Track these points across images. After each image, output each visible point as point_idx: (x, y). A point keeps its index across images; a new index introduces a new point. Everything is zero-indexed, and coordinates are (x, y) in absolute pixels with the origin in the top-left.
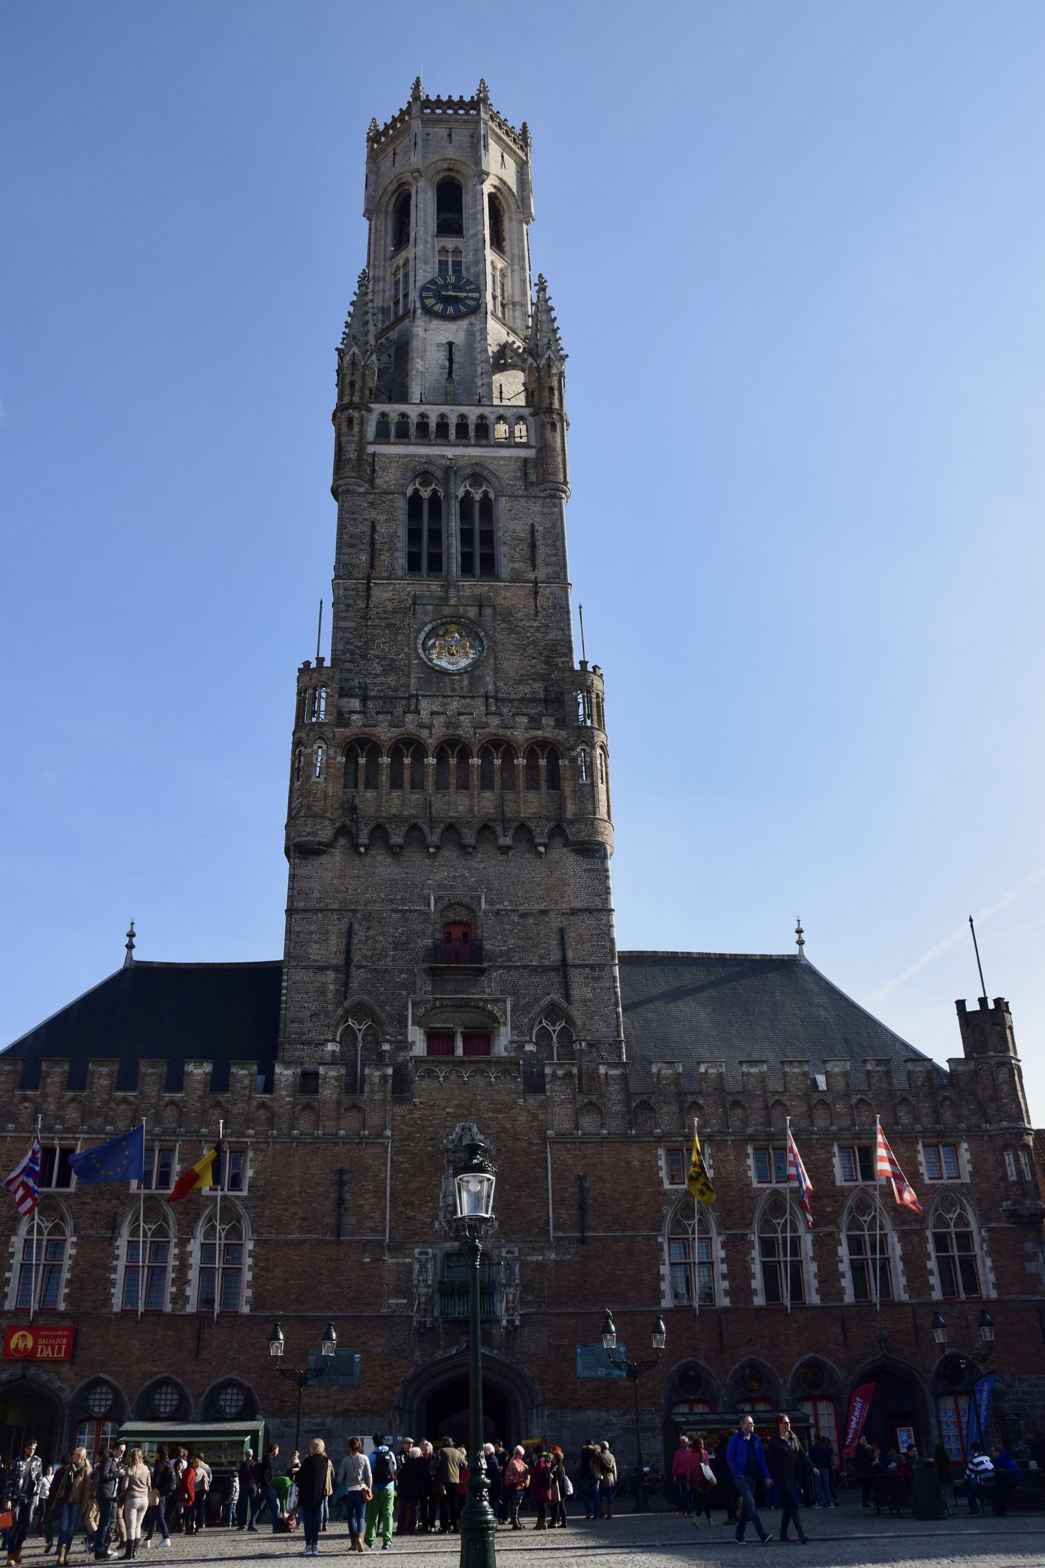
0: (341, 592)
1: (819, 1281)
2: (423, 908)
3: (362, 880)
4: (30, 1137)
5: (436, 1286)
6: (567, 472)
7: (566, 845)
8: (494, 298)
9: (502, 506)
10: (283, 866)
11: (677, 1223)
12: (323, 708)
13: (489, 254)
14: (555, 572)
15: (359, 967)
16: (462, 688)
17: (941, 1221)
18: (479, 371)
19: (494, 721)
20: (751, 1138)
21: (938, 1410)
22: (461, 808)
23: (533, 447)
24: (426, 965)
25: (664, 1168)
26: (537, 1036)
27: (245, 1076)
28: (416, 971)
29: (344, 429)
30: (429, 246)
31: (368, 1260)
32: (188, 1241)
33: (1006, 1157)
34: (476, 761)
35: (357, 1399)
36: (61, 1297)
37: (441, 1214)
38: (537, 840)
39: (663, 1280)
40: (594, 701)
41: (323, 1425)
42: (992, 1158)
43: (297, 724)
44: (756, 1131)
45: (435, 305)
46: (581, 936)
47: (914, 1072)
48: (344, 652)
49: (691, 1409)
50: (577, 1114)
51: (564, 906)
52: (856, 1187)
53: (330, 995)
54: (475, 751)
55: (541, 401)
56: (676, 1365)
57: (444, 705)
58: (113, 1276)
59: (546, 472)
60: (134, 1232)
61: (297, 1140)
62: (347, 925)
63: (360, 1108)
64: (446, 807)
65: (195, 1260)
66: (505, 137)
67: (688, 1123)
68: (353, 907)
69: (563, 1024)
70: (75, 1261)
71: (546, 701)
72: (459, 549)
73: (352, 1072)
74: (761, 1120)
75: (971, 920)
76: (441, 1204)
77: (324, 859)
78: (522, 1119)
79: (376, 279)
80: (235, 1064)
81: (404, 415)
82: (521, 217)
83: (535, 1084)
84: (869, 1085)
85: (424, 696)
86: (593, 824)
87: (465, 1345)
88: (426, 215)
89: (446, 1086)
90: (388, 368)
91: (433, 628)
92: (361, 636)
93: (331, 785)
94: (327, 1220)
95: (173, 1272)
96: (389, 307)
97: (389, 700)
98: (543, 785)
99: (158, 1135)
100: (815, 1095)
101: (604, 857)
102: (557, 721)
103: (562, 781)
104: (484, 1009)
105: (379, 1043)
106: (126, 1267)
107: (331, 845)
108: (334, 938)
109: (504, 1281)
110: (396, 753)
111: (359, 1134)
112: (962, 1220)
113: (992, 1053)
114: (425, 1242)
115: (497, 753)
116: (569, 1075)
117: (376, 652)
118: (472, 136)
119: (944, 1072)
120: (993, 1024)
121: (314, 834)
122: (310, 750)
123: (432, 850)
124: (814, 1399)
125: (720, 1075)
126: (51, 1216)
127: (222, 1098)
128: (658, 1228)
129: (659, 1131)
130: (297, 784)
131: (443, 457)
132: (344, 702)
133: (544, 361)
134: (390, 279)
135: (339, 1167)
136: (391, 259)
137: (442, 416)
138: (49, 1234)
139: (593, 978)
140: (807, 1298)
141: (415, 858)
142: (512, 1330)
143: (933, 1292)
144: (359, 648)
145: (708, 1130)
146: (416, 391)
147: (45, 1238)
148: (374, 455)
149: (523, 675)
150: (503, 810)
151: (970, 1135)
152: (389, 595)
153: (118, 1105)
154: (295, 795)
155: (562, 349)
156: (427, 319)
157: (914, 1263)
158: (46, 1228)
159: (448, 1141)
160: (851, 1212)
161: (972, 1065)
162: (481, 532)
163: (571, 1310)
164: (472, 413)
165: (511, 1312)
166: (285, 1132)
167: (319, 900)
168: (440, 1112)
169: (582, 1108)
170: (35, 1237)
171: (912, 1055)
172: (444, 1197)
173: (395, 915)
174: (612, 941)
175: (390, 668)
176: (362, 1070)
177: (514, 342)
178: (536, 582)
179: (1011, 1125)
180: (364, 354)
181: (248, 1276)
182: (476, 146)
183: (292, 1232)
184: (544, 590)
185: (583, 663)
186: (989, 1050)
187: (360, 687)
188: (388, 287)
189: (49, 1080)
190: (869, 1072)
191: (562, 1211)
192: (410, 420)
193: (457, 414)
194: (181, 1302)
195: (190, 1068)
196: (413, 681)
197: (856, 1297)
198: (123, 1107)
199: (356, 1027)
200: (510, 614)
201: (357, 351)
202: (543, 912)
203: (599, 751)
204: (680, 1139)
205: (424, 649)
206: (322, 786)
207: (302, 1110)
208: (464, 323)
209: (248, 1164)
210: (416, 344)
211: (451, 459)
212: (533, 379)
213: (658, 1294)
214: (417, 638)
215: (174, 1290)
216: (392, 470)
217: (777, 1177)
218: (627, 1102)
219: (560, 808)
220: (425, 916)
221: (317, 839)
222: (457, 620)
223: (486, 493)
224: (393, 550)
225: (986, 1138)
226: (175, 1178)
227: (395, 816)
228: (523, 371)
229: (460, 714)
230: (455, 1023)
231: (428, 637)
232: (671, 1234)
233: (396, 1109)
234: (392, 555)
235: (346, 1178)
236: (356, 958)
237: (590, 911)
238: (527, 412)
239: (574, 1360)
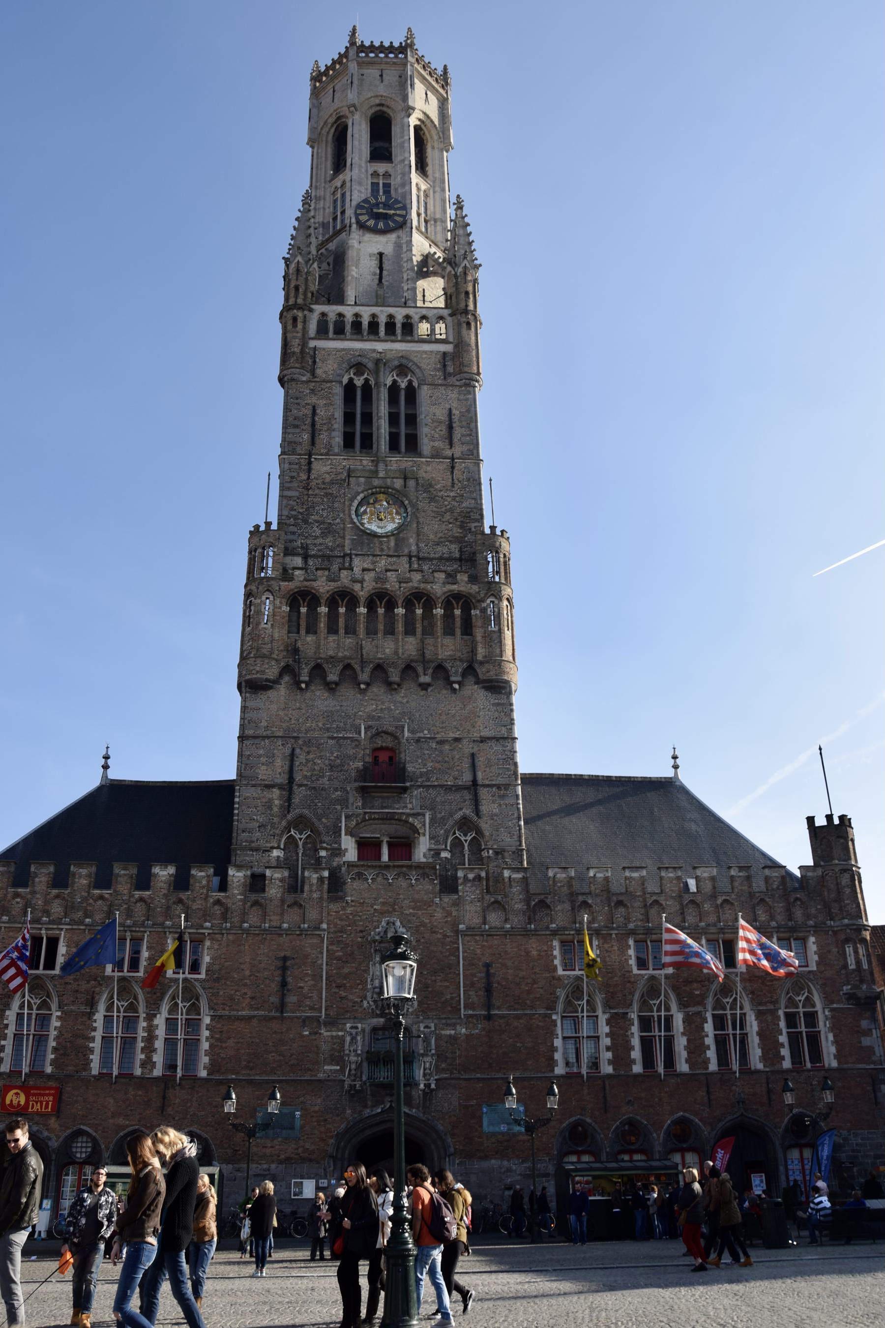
0: (287, 466)
1: (688, 1053)
2: (355, 735)
3: (303, 711)
4: (21, 928)
5: (365, 1055)
6: (481, 364)
7: (477, 683)
8: (419, 215)
9: (424, 393)
10: (236, 699)
11: (568, 1003)
12: (270, 565)
13: (415, 177)
14: (469, 450)
15: (300, 786)
16: (389, 548)
17: (791, 1003)
18: (405, 277)
19: (417, 577)
20: (632, 932)
21: (786, 1161)
22: (387, 651)
23: (450, 343)
24: (357, 784)
25: (558, 957)
26: (451, 845)
27: (203, 877)
28: (348, 789)
29: (290, 327)
30: (363, 170)
31: (307, 1033)
32: (155, 1016)
33: (847, 949)
34: (400, 611)
35: (297, 1149)
36: (48, 1062)
37: (369, 995)
38: (453, 679)
39: (557, 1051)
40: (502, 560)
41: (269, 1170)
42: (835, 950)
43: (248, 578)
44: (636, 926)
46: (489, 760)
47: (771, 877)
48: (289, 517)
49: (579, 1158)
50: (485, 911)
51: (475, 734)
53: (275, 809)
54: (400, 602)
55: (458, 303)
56: (567, 1122)
57: (374, 563)
58: (91, 1045)
59: (462, 364)
60: (109, 1008)
61: (247, 931)
62: (290, 750)
63: (301, 905)
64: (375, 650)
65: (161, 1032)
66: (428, 78)
67: (578, 919)
68: (295, 735)
70: (60, 1031)
71: (460, 560)
72: (387, 429)
73: (294, 875)
74: (641, 917)
75: (820, 749)
76: (369, 986)
77: (271, 694)
78: (439, 915)
79: (318, 199)
80: (194, 867)
81: (340, 315)
82: (442, 146)
83: (449, 885)
84: (733, 888)
85: (356, 555)
86: (500, 665)
87: (388, 1105)
88: (360, 144)
89: (374, 887)
90: (328, 274)
91: (365, 497)
92: (303, 504)
93: (277, 630)
94: (272, 999)
95: (142, 1041)
96: (329, 222)
98: (458, 631)
99: (129, 927)
100: (686, 896)
101: (510, 693)
102: (469, 577)
103: (474, 629)
104: (406, 822)
105: (316, 850)
106: (103, 1037)
107: (276, 682)
108: (279, 761)
109: (422, 1051)
110: (333, 603)
111: (299, 927)
112: (809, 1001)
113: (837, 862)
114: (355, 1018)
115: (419, 603)
116: (478, 878)
117: (316, 518)
118: (400, 77)
119: (796, 877)
120: (838, 837)
121: (263, 672)
122: (258, 601)
123: (363, 686)
124: (683, 1151)
125: (606, 879)
126: (39, 994)
127: (184, 896)
128: (552, 1007)
129: (554, 925)
130: (248, 629)
131: (374, 351)
132: (288, 559)
133: (460, 269)
134: (329, 199)
135: (282, 955)
136: (330, 181)
137: (374, 316)
138: (38, 1009)
139: (499, 796)
140: (678, 1066)
141: (347, 692)
142: (428, 1093)
143: (783, 1062)
144: (301, 514)
145: (596, 925)
146: (351, 294)
147: (34, 1012)
148: (315, 348)
149: (441, 538)
150: (424, 653)
151: (818, 930)
152: (328, 468)
153: (95, 901)
154: (246, 639)
155: (476, 259)
156: (361, 232)
157: (768, 1038)
158: (35, 1004)
159: (375, 934)
160: (716, 995)
161: (819, 872)
162: (406, 415)
163: (478, 1075)
164: (399, 314)
165: (428, 1077)
166: (237, 925)
167: (267, 728)
168: (369, 909)
169: (488, 906)
170: (26, 1011)
171: (769, 863)
172: (372, 980)
173: (331, 742)
174: (516, 765)
175: (328, 531)
176: (303, 873)
177: (435, 253)
178: (453, 459)
179: (851, 922)
180: (307, 262)
181: (205, 1045)
182: (403, 85)
183: (243, 1009)
184: (460, 465)
185: (493, 528)
186: (833, 859)
187: (302, 547)
188: (327, 205)
189: (37, 880)
190: (732, 877)
192: (346, 320)
193: (386, 314)
194: (149, 1067)
195: (156, 870)
196: (347, 542)
197: (719, 1065)
198: (100, 902)
199: (297, 836)
200: (431, 485)
201: (301, 260)
202: (457, 740)
203: (505, 603)
204: (572, 932)
205: (357, 515)
206: (269, 631)
207: (252, 906)
208: (392, 237)
209: (206, 951)
210: (351, 254)
211: (381, 353)
212: (452, 285)
213: (552, 1063)
214: (350, 505)
215: (143, 1056)
216: (330, 362)
217: (654, 965)
218: (527, 901)
219: (472, 651)
220: (357, 743)
221: (265, 677)
222: (385, 490)
223: (410, 382)
224: (330, 430)
225: (830, 933)
226: (143, 963)
227: (332, 657)
228: (443, 277)
229: (387, 571)
230: (381, 833)
231: (360, 504)
232: (564, 1012)
233: (331, 906)
234: (330, 434)
235: (288, 963)
236: (298, 777)
237: (497, 739)
238: (446, 313)
239: (481, 1118)
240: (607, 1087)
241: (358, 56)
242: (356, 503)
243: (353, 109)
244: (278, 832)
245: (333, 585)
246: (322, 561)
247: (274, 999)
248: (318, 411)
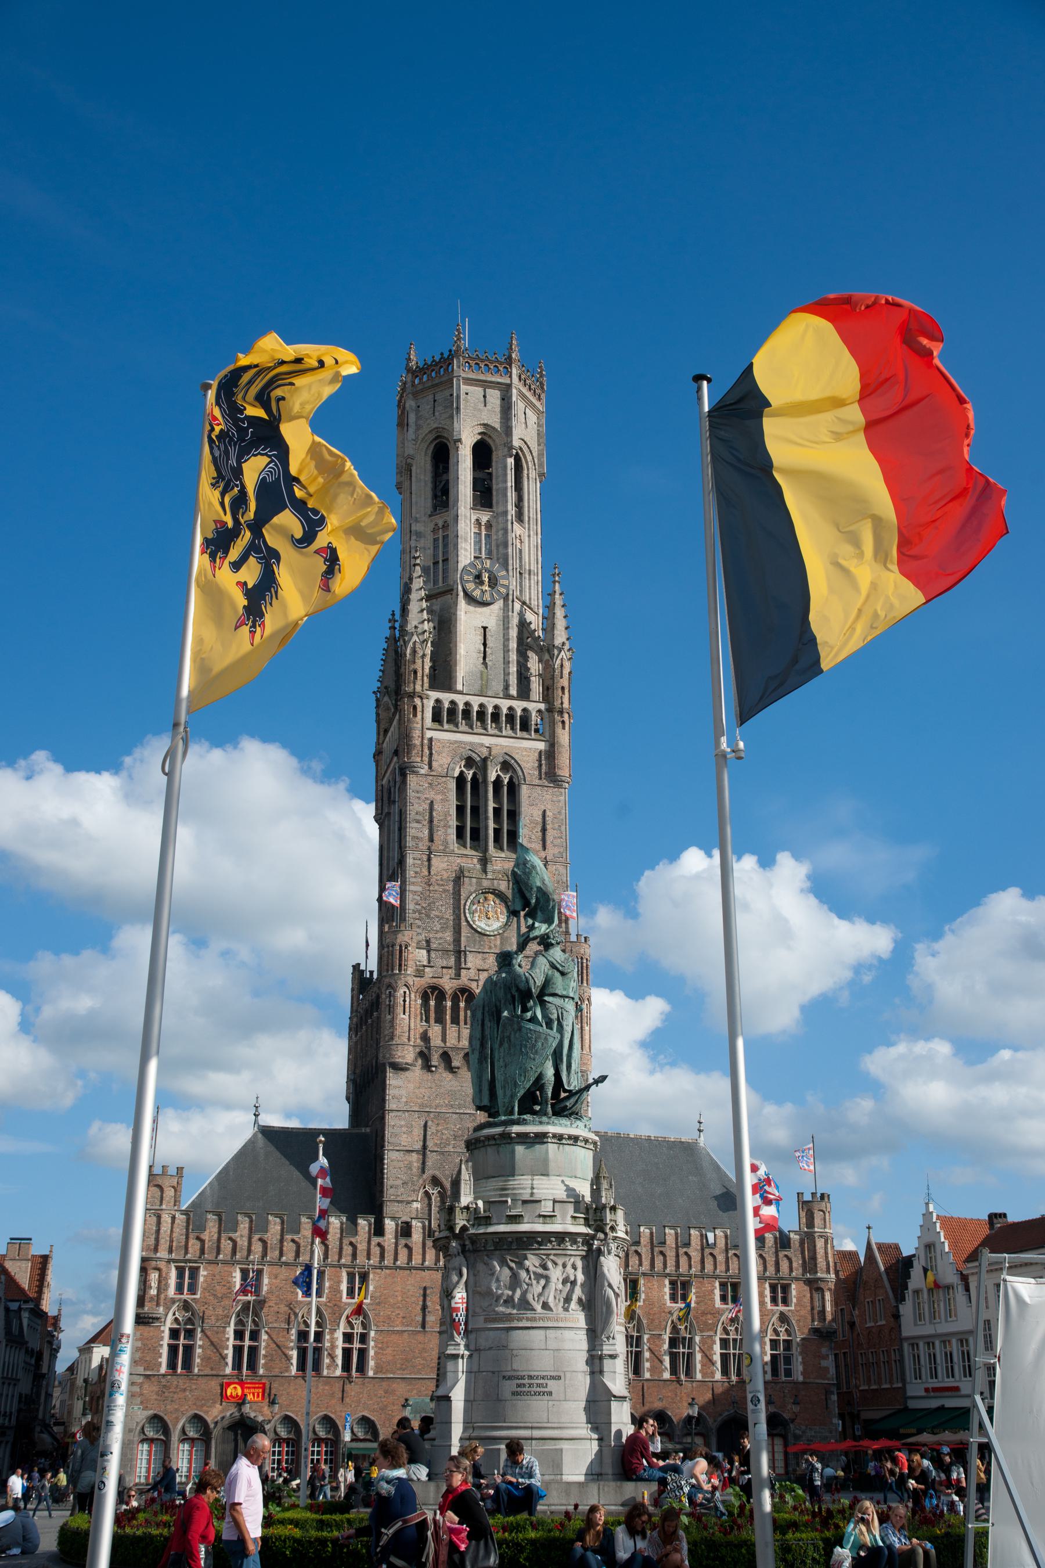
9: (524, 791)
16: (495, 946)
45: (474, 590)
53: (415, 1170)
57: (484, 959)
58: (291, 1353)
65: (340, 1343)
68: (427, 1110)
81: (453, 702)
92: (425, 899)
96: (429, 566)
110: (455, 999)
117: (437, 913)
121: (403, 1057)
131: (482, 745)
133: (558, 662)
134: (430, 538)
148: (431, 740)
151: (797, 1279)
152: (444, 865)
164: (505, 705)
183: (397, 1326)
189: (242, 1226)
196: (463, 939)
199: (431, 1192)
203: (586, 1002)
205: (470, 913)
214: (465, 904)
216: (444, 755)
221: (405, 1061)
223: (511, 778)
231: (472, 903)
235: (428, 1292)
236: (430, 1144)
240: (645, 1388)
244: (416, 1188)
245: (455, 984)
247: (420, 1318)
248: (436, 807)
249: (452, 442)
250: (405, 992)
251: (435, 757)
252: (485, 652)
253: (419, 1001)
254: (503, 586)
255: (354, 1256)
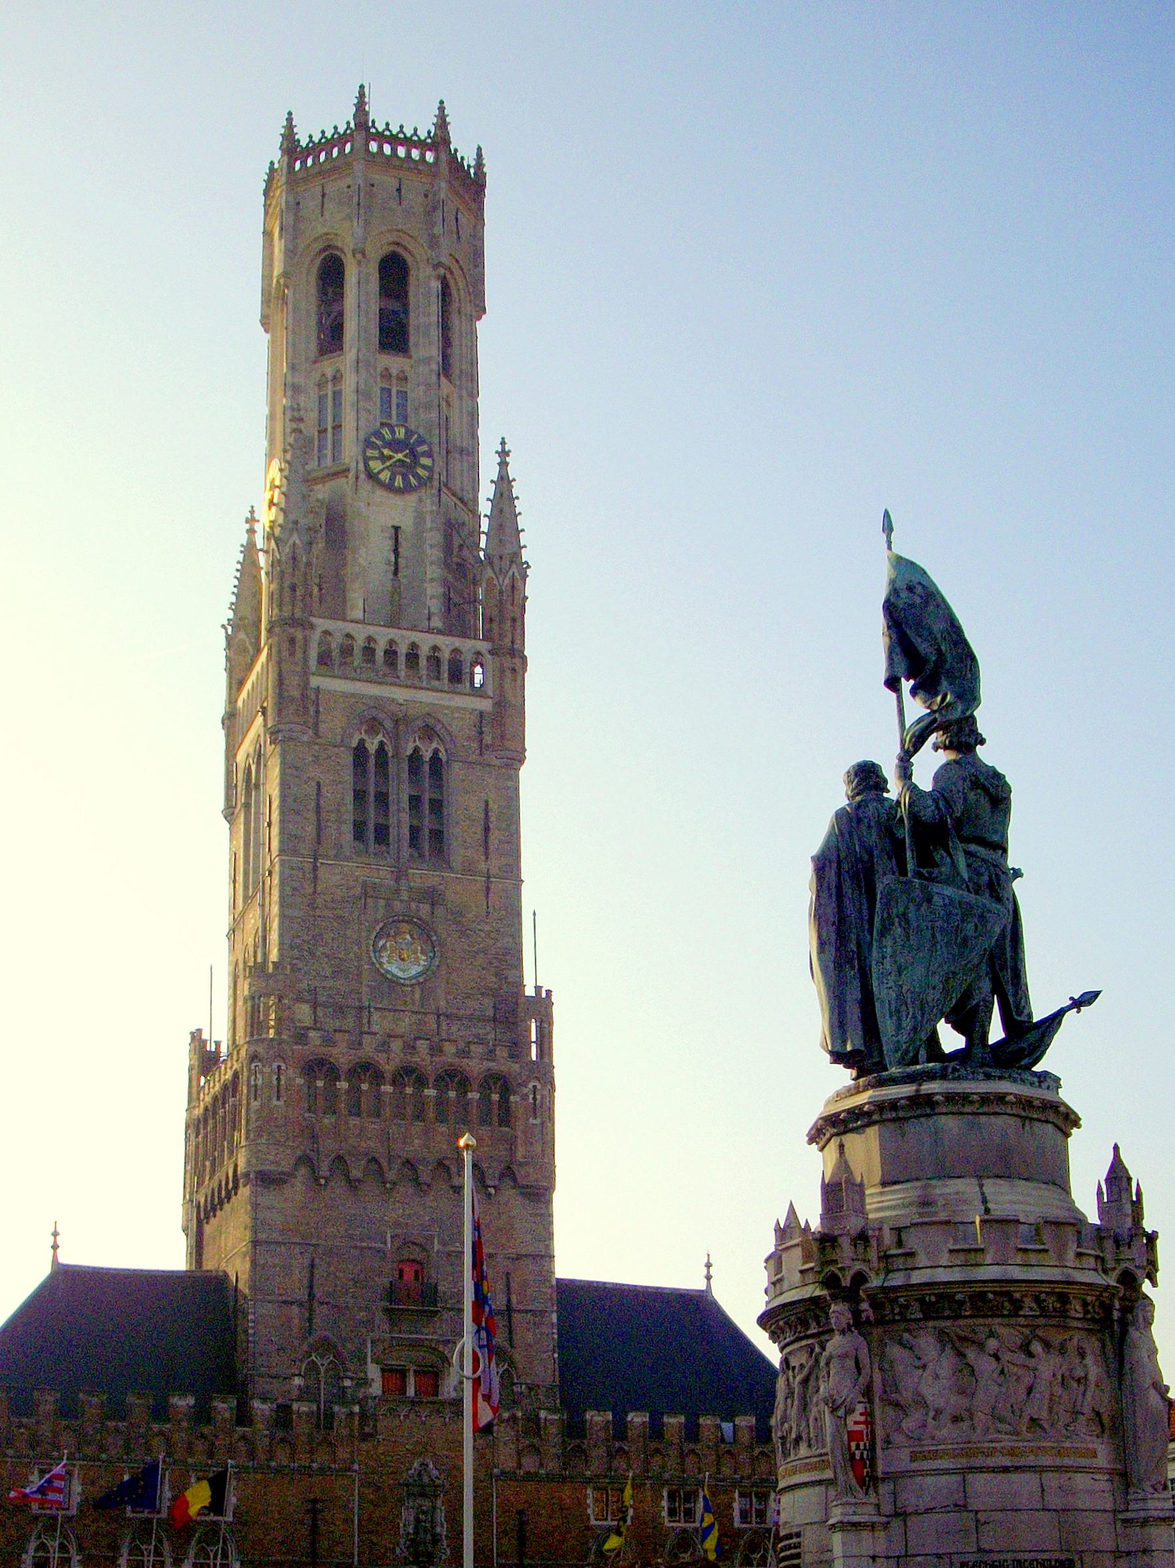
0: (287, 871)
2: (379, 1245)
15: (322, 1303)
18: (429, 576)
23: (489, 697)
24: (383, 1304)
29: (285, 654)
32: (182, 1561)
37: (402, 1541)
44: (672, 1475)
50: (519, 1453)
52: (750, 1529)
54: (431, 1081)
55: (502, 636)
68: (314, 1242)
69: (506, 1367)
71: (494, 1020)
76: (402, 1531)
81: (349, 636)
85: (376, 1009)
97: (340, 1010)
101: (549, 1202)
104: (434, 1349)
107: (291, 1175)
116: (513, 1418)
118: (426, 196)
121: (277, 1163)
131: (393, 700)
133: (507, 581)
134: (314, 393)
135: (312, 1496)
164: (426, 642)
172: (404, 1526)
178: (489, 878)
184: (496, 885)
185: (538, 989)
187: (309, 991)
191: (505, 1541)
196: (364, 989)
205: (375, 952)
208: (411, 499)
211: (401, 705)
214: (368, 938)
223: (436, 751)
224: (340, 821)
231: (379, 936)
236: (318, 1292)
238: (483, 646)
241: (367, 150)
242: (373, 937)
243: (359, 256)
246: (334, 1011)
248: (324, 790)
249: (350, 255)
250: (279, 1067)
251: (322, 717)
252: (396, 563)
253: (300, 1081)
254: (424, 467)
255: (211, 1454)
